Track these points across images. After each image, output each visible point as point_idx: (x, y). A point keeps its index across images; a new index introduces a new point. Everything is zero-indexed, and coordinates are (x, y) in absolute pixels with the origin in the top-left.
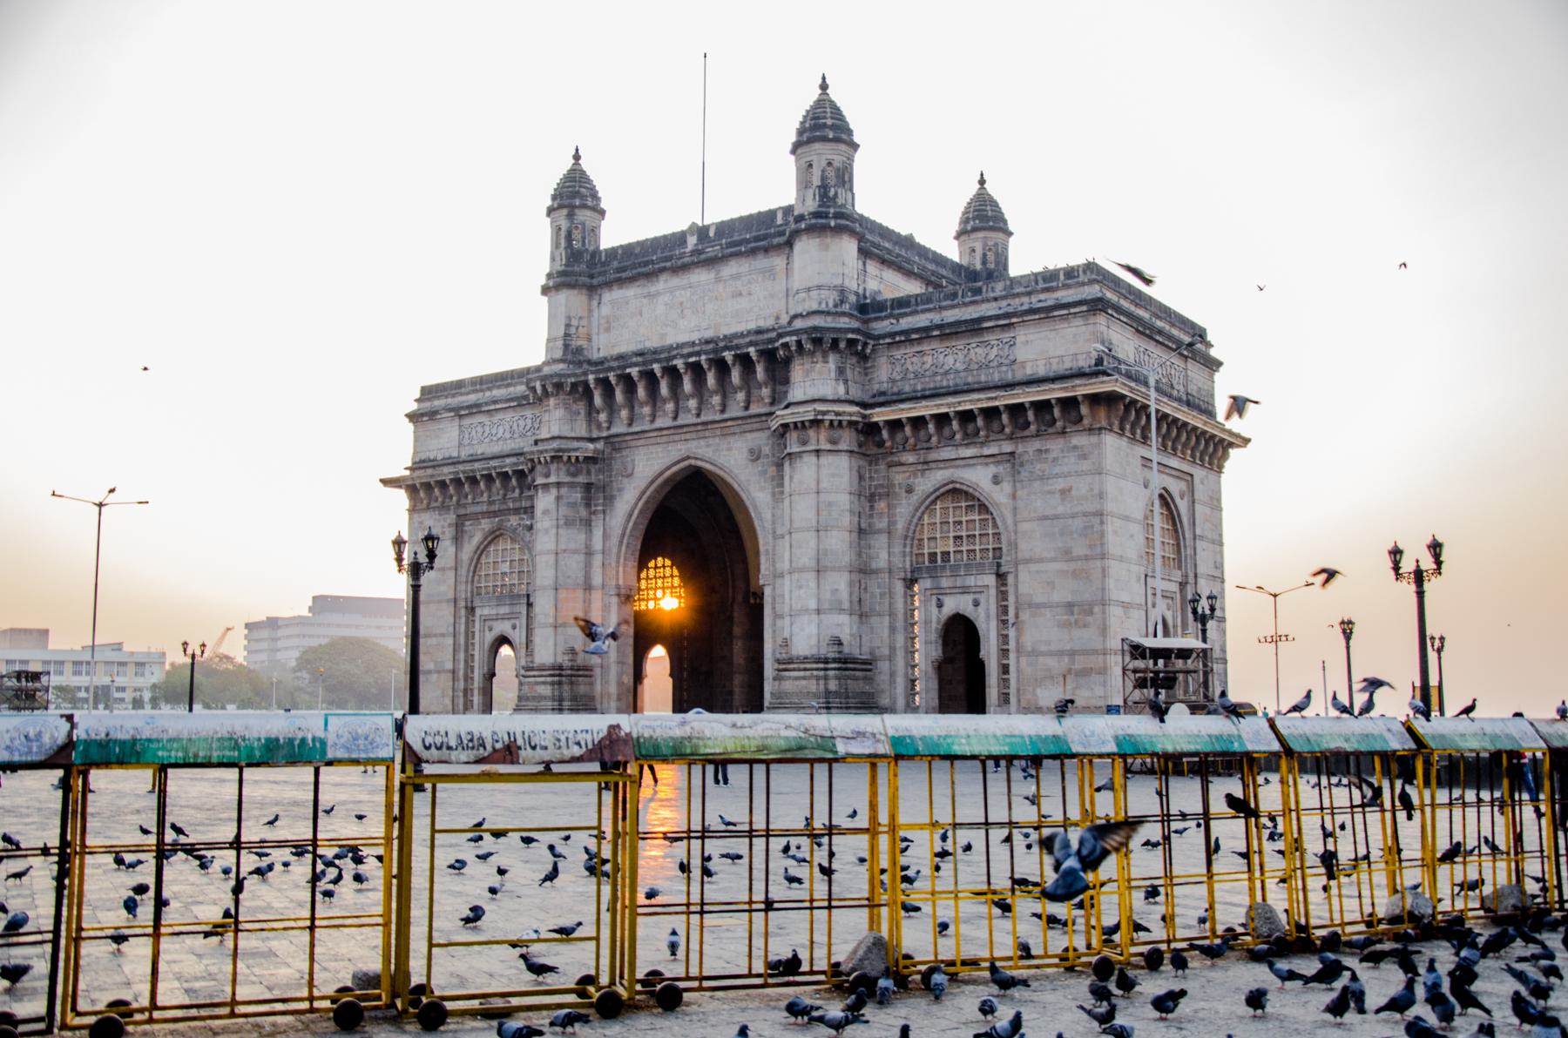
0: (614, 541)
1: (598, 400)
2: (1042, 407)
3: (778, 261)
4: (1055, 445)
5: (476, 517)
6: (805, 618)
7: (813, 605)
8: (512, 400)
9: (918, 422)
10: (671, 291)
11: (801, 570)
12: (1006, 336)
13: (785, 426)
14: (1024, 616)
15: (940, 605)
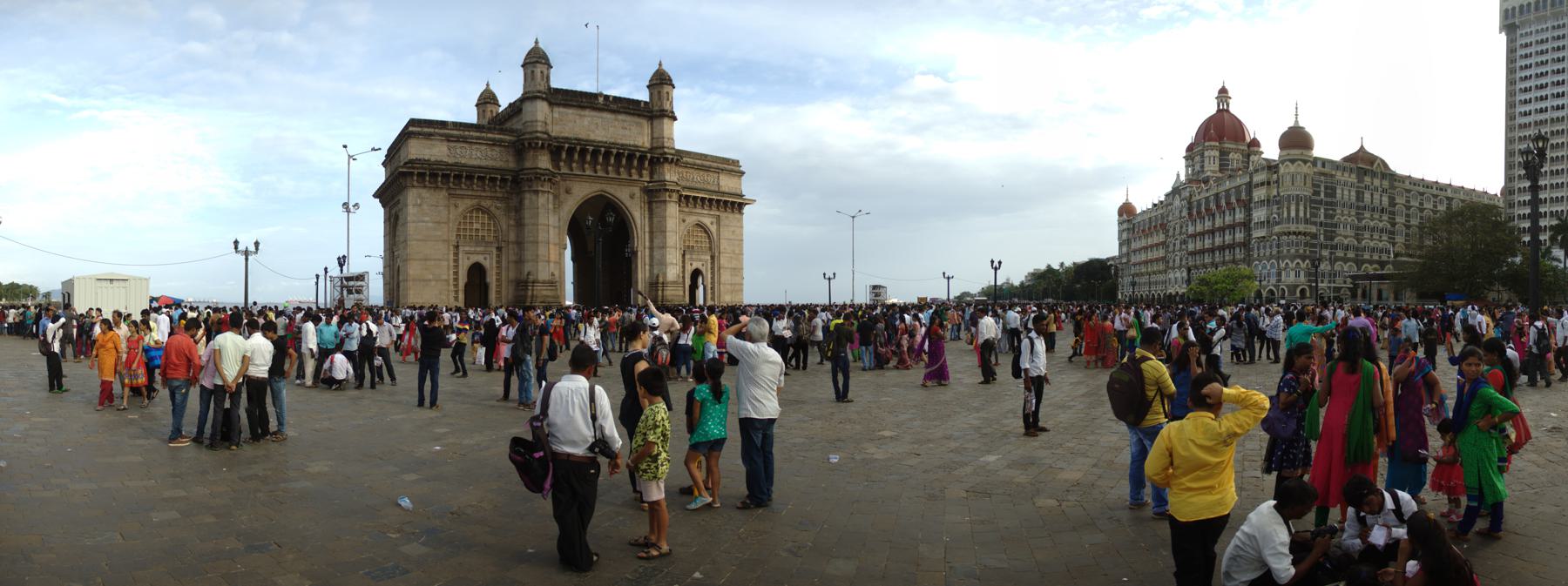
0: (561, 223)
1: (564, 155)
2: (733, 203)
3: (645, 123)
4: (731, 216)
5: (462, 197)
6: (672, 266)
7: (675, 262)
8: (489, 139)
9: (695, 198)
10: (592, 117)
11: (671, 247)
12: (716, 175)
13: (667, 190)
14: (721, 271)
15: (691, 265)
